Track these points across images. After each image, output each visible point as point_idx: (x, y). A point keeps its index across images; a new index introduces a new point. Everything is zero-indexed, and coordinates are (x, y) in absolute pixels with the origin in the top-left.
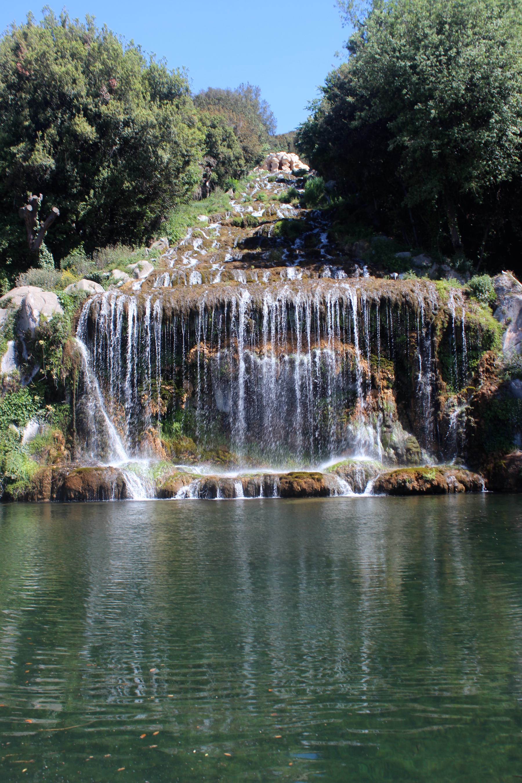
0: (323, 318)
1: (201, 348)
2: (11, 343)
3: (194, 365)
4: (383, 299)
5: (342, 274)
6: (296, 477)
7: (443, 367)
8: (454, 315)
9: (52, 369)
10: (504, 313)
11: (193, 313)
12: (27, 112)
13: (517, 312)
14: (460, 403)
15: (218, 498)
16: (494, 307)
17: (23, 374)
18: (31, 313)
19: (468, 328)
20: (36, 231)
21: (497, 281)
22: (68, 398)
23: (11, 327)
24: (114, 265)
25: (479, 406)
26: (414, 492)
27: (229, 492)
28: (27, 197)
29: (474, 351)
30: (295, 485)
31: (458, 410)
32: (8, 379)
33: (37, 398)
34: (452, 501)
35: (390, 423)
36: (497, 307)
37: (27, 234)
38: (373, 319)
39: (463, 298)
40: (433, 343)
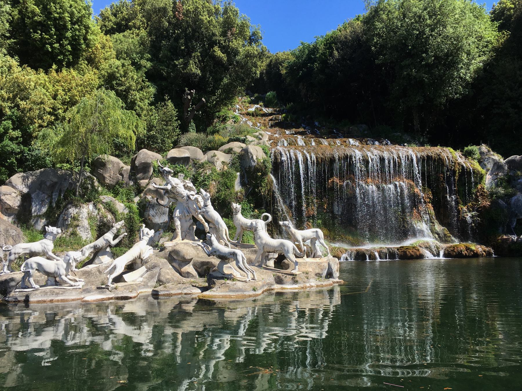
1: (336, 180)
2: (238, 174)
3: (332, 189)
5: (377, 143)
7: (457, 192)
8: (464, 165)
9: (261, 189)
10: (485, 165)
11: (332, 160)
12: (182, 41)
13: (492, 165)
14: (470, 211)
15: (368, 260)
16: (480, 162)
17: (246, 191)
18: (252, 157)
19: (474, 172)
21: (480, 149)
22: (264, 205)
23: (238, 164)
24: (246, 133)
25: (482, 212)
26: (466, 257)
27: (372, 257)
28: (185, 90)
29: (476, 184)
30: (408, 253)
31: (469, 215)
33: (252, 205)
34: (481, 260)
36: (482, 162)
38: (423, 166)
39: (463, 157)
40: (454, 179)
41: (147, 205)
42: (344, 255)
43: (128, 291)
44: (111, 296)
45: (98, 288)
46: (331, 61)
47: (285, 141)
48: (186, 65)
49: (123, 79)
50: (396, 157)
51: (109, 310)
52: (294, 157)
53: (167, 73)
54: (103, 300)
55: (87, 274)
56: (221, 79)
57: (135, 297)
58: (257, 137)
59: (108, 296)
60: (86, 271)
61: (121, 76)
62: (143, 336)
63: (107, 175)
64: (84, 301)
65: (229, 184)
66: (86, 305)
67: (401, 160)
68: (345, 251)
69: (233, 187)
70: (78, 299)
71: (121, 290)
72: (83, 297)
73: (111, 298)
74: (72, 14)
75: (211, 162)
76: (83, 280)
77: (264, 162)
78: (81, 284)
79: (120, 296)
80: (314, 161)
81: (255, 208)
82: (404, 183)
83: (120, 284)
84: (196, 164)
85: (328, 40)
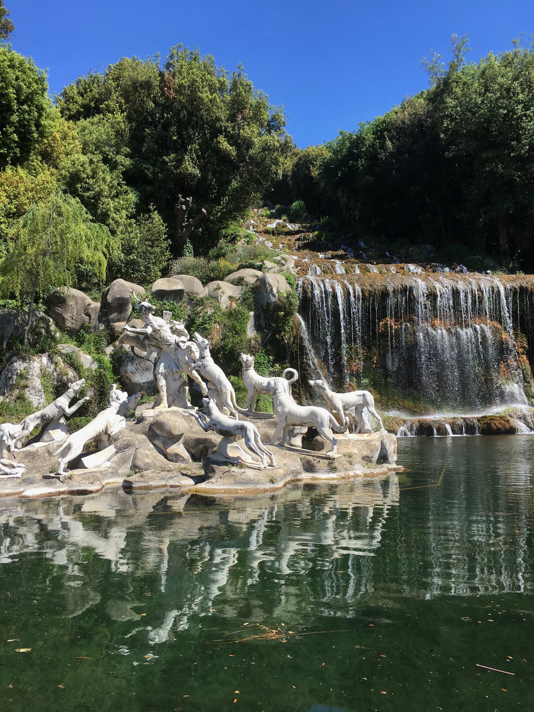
0: (481, 302)
1: (390, 321)
2: (252, 313)
3: (384, 335)
4: (521, 288)
5: (447, 269)
6: (491, 419)
9: (285, 335)
11: (385, 294)
12: (174, 129)
18: (272, 290)
20: (183, 227)
22: (289, 357)
23: (251, 300)
24: (263, 257)
27: (442, 431)
28: (178, 198)
30: (493, 425)
32: (253, 342)
33: (271, 358)
35: (528, 380)
37: (176, 228)
38: (514, 302)
41: (124, 357)
42: (403, 428)
43: (87, 482)
44: (62, 490)
45: (45, 477)
46: (382, 156)
47: (318, 268)
48: (180, 161)
49: (91, 181)
50: (475, 288)
51: (61, 509)
52: (331, 290)
53: (155, 174)
54: (50, 494)
55: (32, 456)
56: (229, 182)
57: (97, 491)
58: (278, 263)
59: (58, 490)
60: (30, 452)
61: (88, 177)
62: (111, 548)
63: (67, 316)
64: (23, 497)
65: (238, 328)
66: (25, 501)
67: (482, 292)
68: (402, 423)
69: (245, 332)
70: (15, 494)
71: (78, 480)
72: (22, 490)
73: (63, 493)
74: (18, 90)
75: (214, 297)
76: (23, 465)
77: (288, 297)
78: (20, 471)
79: (75, 489)
80: (359, 295)
81: (275, 361)
82: (487, 327)
83: (76, 472)
84: (193, 300)
85: (379, 126)
